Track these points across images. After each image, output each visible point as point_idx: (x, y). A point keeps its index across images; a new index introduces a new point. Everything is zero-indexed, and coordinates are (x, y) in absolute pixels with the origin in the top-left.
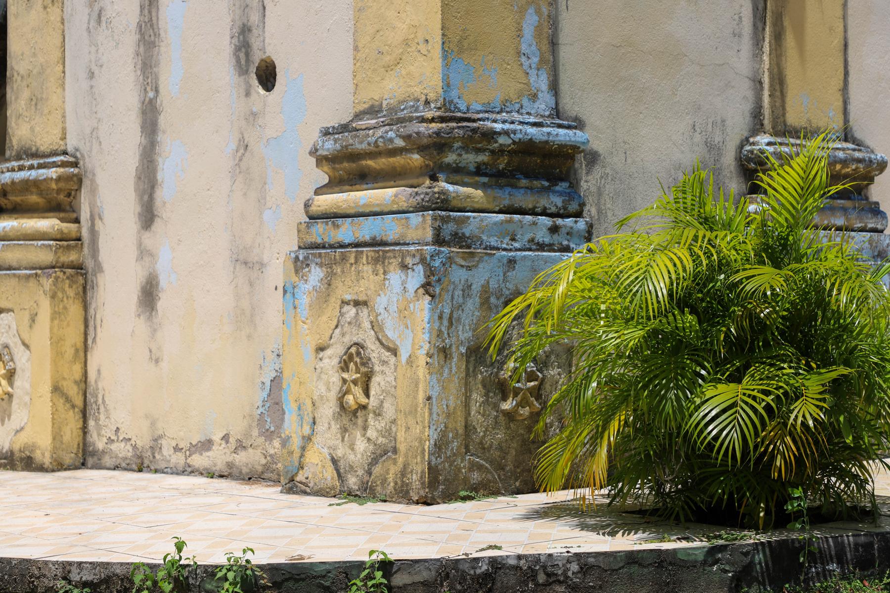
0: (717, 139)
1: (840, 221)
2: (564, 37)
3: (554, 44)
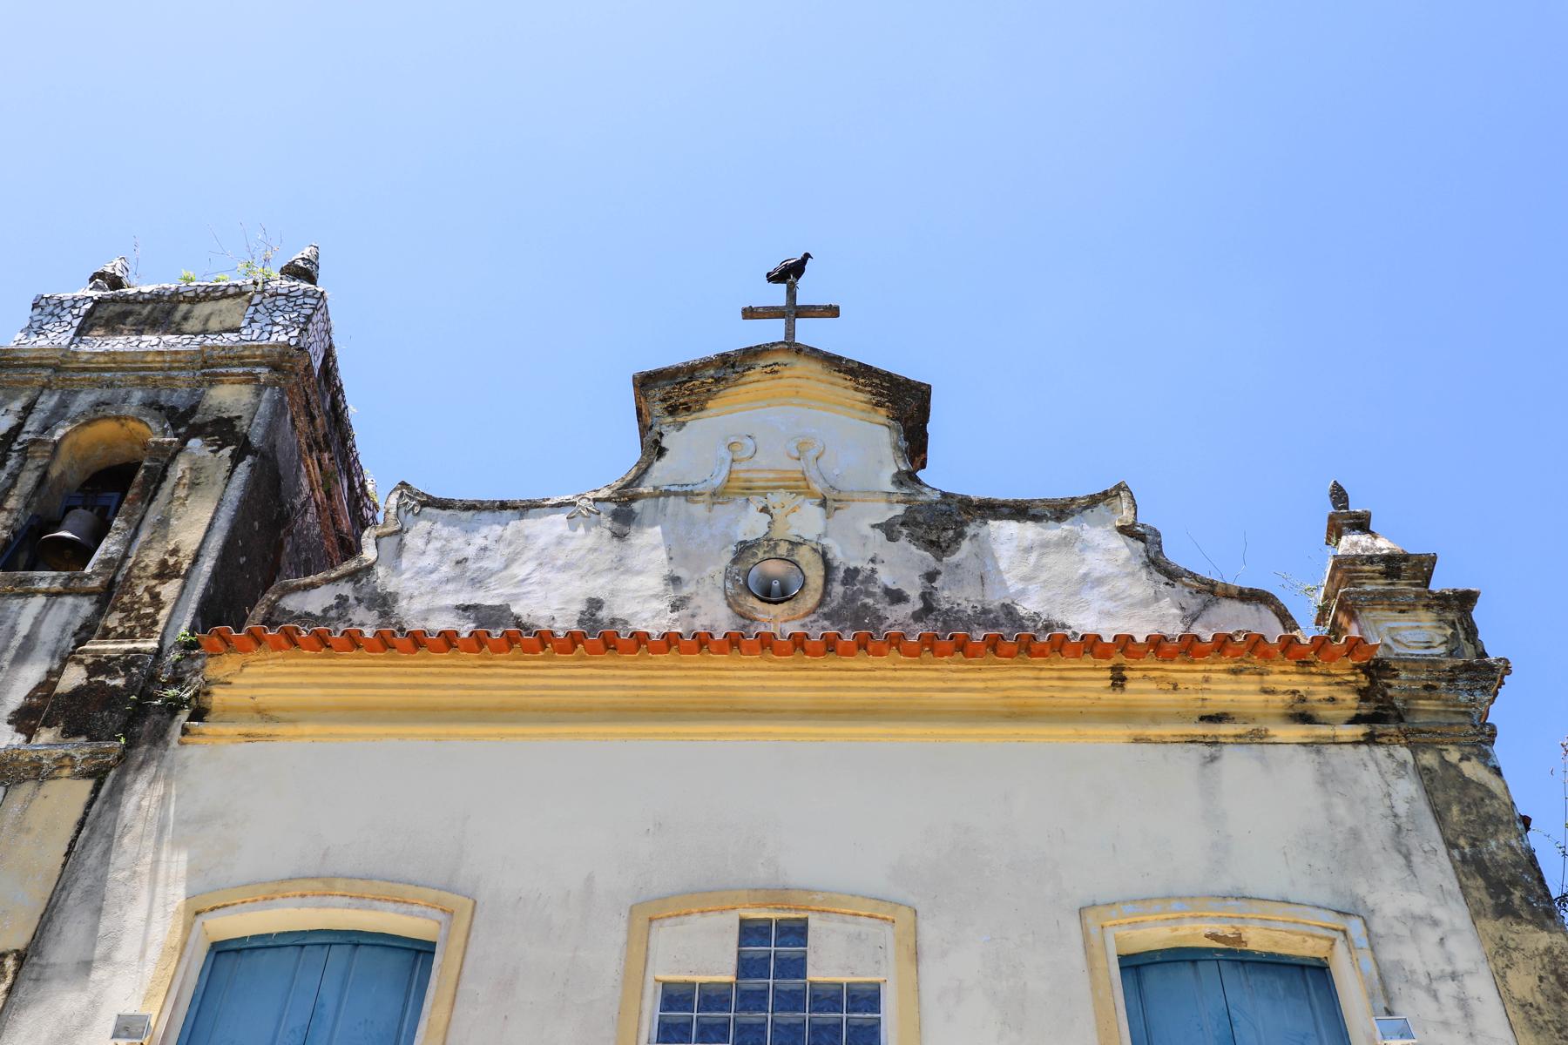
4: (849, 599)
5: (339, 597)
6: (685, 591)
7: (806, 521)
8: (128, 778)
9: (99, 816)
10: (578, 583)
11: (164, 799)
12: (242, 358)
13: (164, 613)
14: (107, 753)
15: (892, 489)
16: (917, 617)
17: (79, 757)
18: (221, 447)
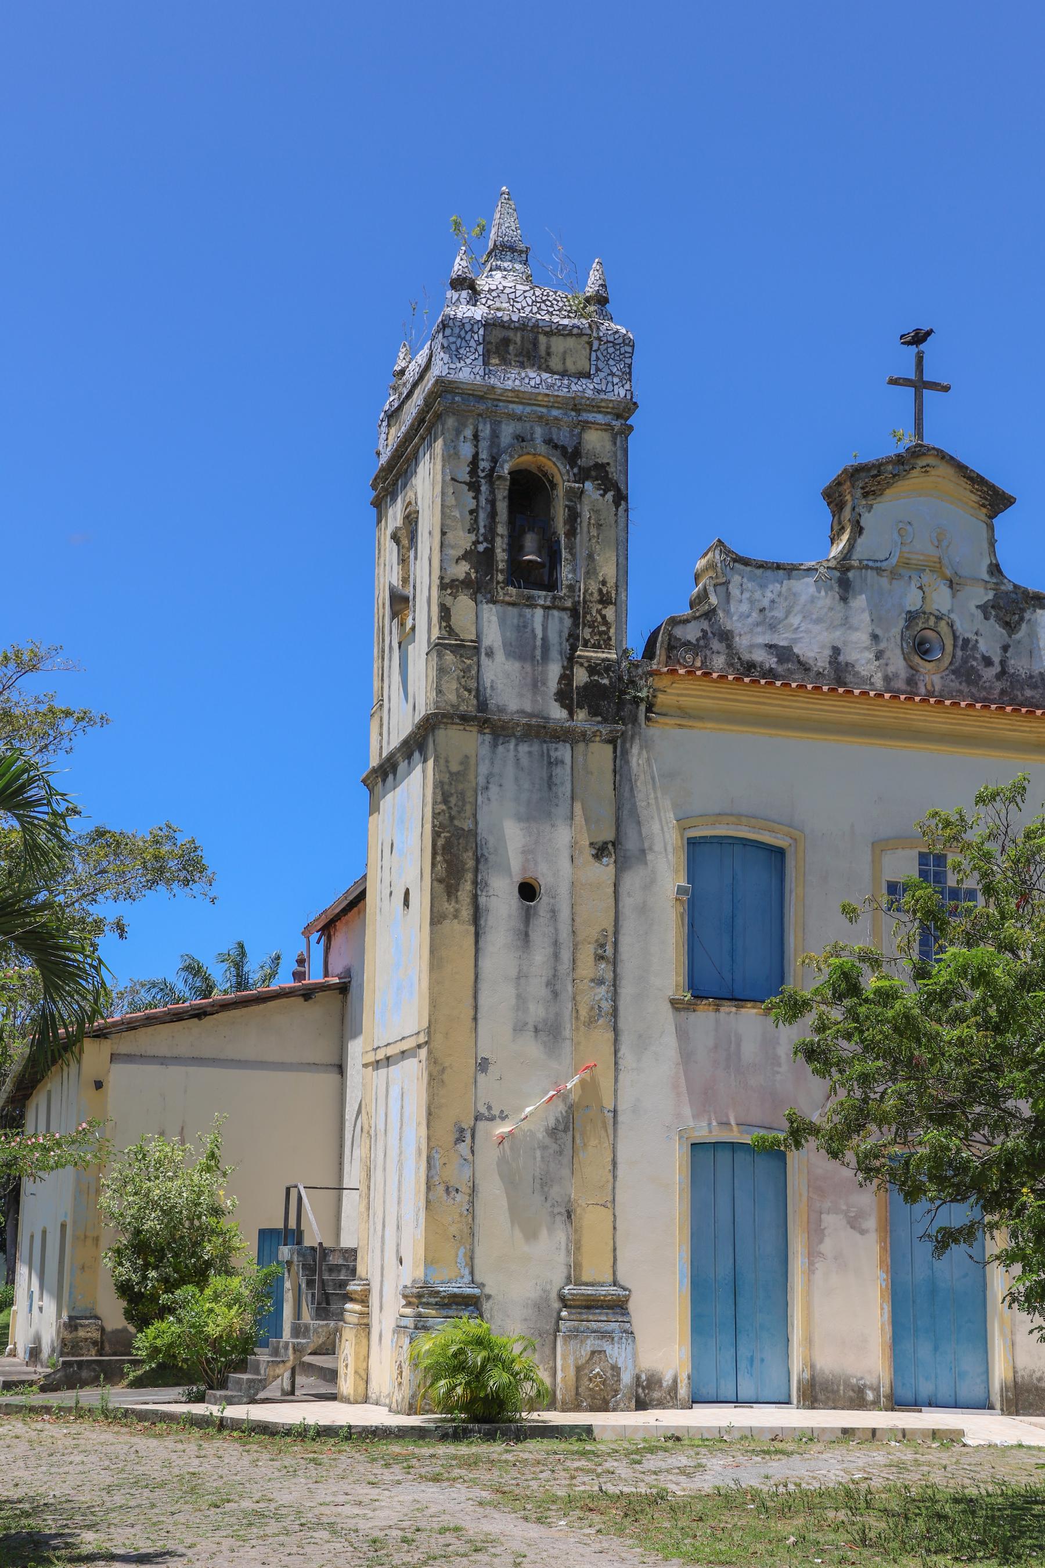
0: (548, 1287)
1: (605, 1319)
2: (476, 1256)
3: (472, 1258)
4: (965, 661)
5: (702, 630)
6: (883, 645)
7: (941, 599)
8: (628, 745)
9: (621, 767)
10: (826, 634)
11: (648, 759)
12: (599, 407)
13: (612, 631)
14: (617, 731)
15: (986, 577)
16: (999, 676)
17: (604, 732)
18: (605, 492)
